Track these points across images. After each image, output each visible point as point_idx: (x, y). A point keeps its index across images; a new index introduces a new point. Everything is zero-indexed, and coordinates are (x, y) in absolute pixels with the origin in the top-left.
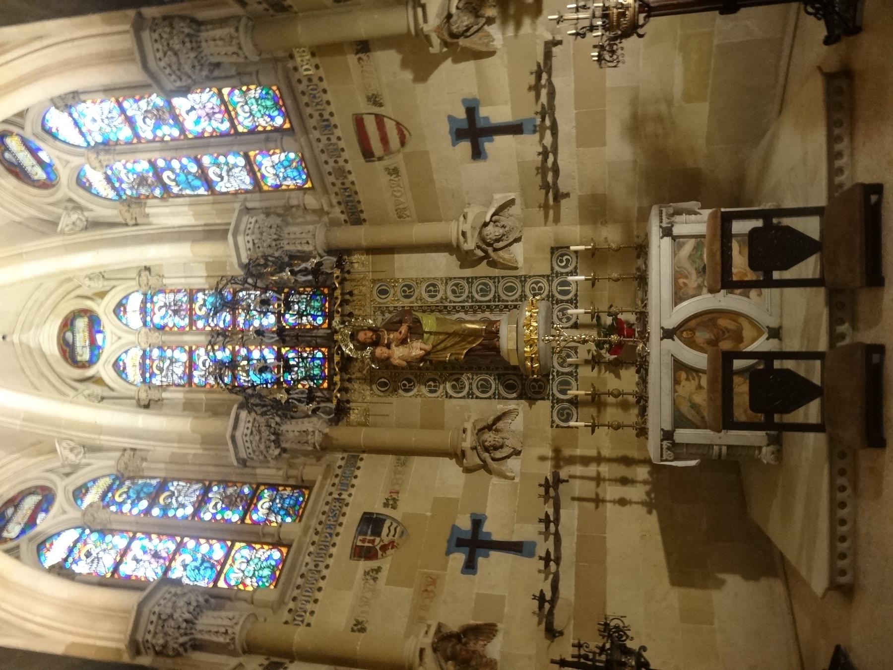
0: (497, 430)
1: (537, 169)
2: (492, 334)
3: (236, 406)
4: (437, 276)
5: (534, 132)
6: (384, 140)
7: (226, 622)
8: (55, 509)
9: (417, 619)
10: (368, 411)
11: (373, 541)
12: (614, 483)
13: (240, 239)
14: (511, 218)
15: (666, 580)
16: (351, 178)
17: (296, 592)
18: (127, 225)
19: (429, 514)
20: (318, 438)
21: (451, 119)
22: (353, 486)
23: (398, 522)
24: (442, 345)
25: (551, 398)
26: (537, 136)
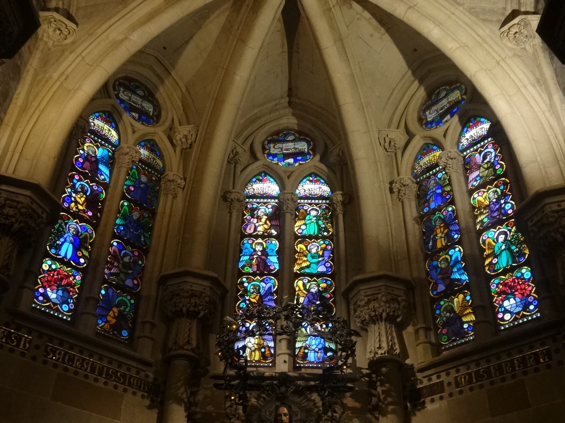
8: (138, 125)
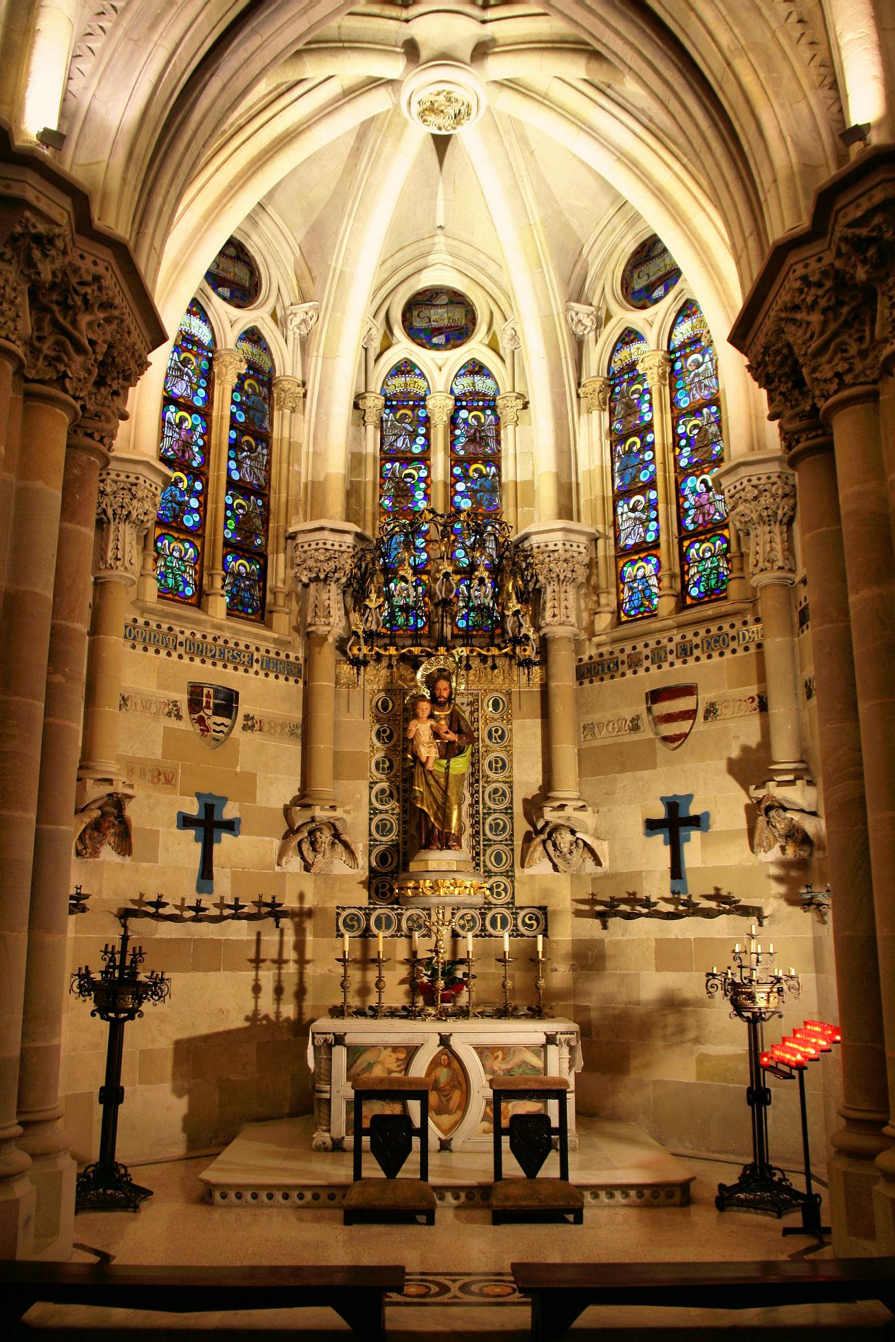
0: (333, 844)
1: (634, 894)
2: (446, 841)
3: (359, 530)
4: (515, 773)
5: (673, 892)
6: (670, 718)
7: (127, 558)
9: (132, 766)
10: (354, 687)
11: (208, 708)
12: (276, 978)
13: (559, 536)
14: (581, 861)
15: (179, 1036)
16: (629, 673)
17: (153, 625)
18: (579, 385)
19: (238, 769)
20: (323, 630)
21: (689, 798)
22: (267, 675)
23: (228, 734)
24: (432, 782)
25: (371, 906)
26: (668, 895)
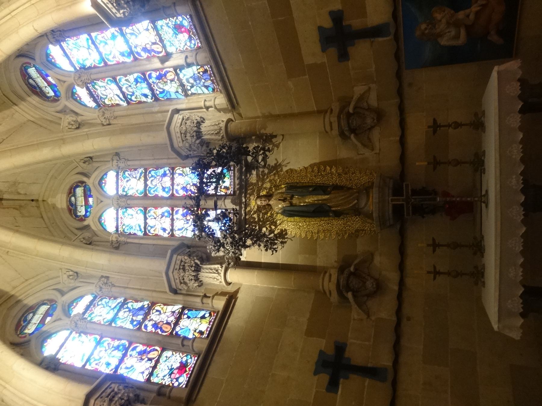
3: (169, 251)
